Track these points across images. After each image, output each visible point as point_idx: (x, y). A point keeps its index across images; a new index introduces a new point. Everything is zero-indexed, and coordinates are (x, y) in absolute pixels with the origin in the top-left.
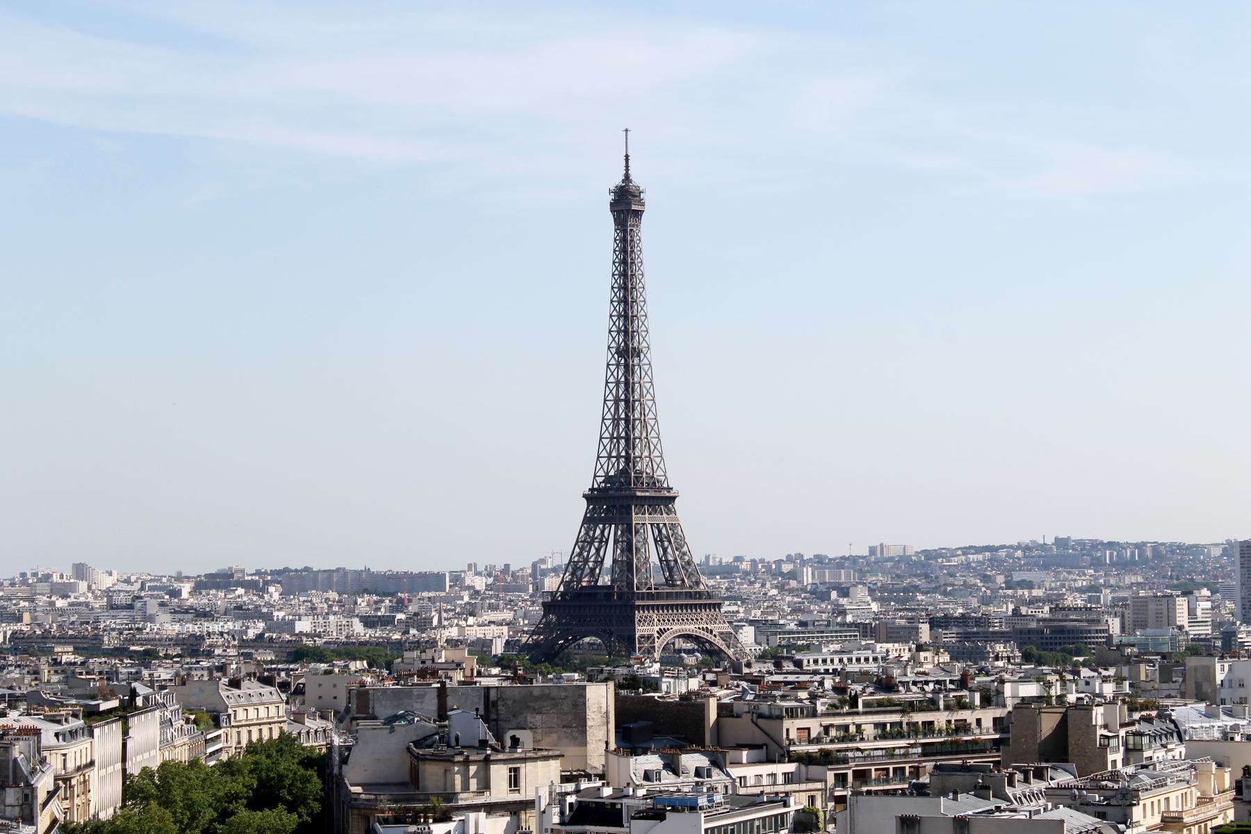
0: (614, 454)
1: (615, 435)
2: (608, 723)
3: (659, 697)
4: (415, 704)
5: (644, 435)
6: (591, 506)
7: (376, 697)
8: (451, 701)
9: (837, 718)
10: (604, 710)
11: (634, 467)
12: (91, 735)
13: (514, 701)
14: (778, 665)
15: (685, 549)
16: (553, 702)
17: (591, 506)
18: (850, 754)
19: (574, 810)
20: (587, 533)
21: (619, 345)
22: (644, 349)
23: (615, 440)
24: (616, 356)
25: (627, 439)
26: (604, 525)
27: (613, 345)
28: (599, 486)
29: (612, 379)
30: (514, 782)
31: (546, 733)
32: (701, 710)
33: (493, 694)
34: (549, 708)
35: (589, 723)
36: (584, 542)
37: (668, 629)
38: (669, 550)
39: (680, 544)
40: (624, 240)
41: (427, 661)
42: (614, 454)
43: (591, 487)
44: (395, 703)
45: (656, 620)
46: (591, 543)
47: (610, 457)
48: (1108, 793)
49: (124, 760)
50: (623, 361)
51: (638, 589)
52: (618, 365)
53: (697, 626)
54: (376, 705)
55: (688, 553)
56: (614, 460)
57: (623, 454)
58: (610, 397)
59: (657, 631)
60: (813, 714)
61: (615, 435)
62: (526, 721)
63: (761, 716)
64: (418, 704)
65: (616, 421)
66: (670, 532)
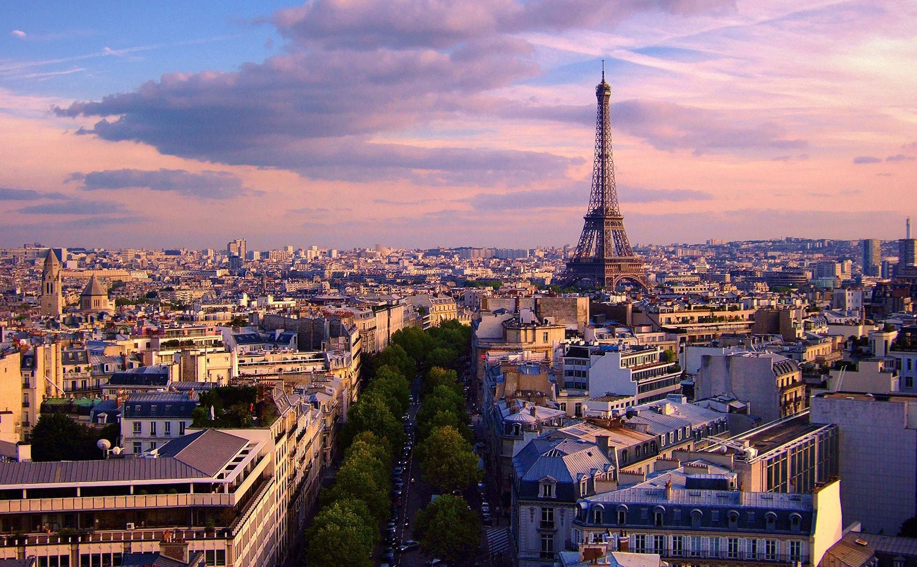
0: (597, 200)
2: (586, 314)
12: (375, 316)
15: (626, 241)
18: (688, 329)
20: (585, 234)
25: (602, 193)
29: (596, 168)
30: (546, 338)
32: (625, 309)
36: (584, 238)
39: (624, 238)
40: (602, 108)
42: (597, 200)
47: (595, 201)
48: (792, 347)
49: (389, 326)
52: (599, 162)
58: (595, 176)
60: (672, 312)
63: (650, 312)
65: (598, 186)
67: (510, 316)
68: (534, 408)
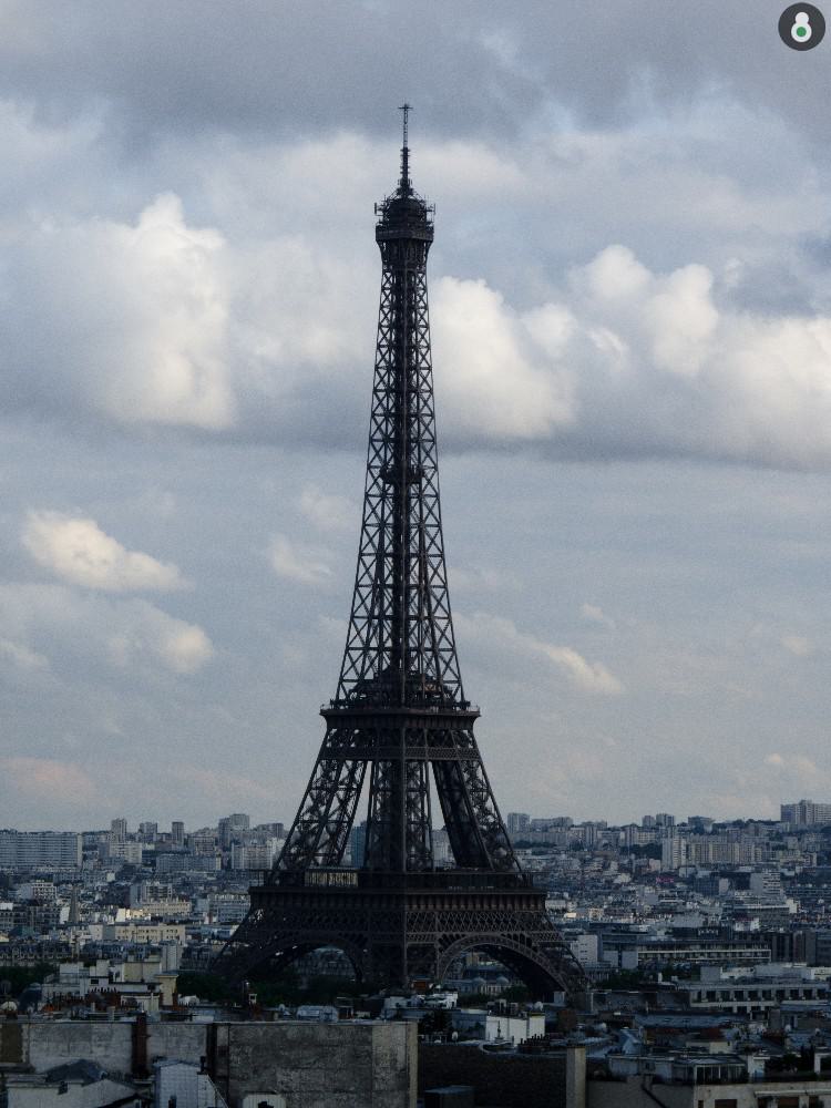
0: (374, 644)
1: (376, 612)
2: (405, 1086)
4: (94, 1049)
6: (334, 731)
7: (33, 1035)
8: (154, 1046)
9: (781, 1085)
10: (400, 1066)
11: (407, 665)
13: (257, 1048)
15: (489, 804)
16: (320, 1050)
17: (334, 731)
20: (326, 775)
21: (386, 463)
22: (427, 471)
23: (376, 621)
24: (380, 481)
25: (396, 619)
26: (355, 762)
27: (377, 462)
28: (348, 696)
29: (373, 520)
31: (307, 1100)
33: (222, 1034)
34: (312, 1061)
36: (321, 790)
37: (458, 937)
40: (397, 289)
41: (101, 981)
42: (374, 644)
43: (334, 698)
44: (63, 1046)
45: (438, 921)
46: (332, 792)
47: (366, 648)
50: (391, 491)
51: (408, 869)
52: (383, 496)
54: (32, 1049)
55: (493, 812)
56: (373, 654)
57: (389, 644)
58: (370, 549)
59: (440, 941)
60: (743, 1078)
61: (376, 612)
63: (658, 1080)
64: (102, 1049)
65: (378, 588)
66: (466, 776)
67: (119, 1091)
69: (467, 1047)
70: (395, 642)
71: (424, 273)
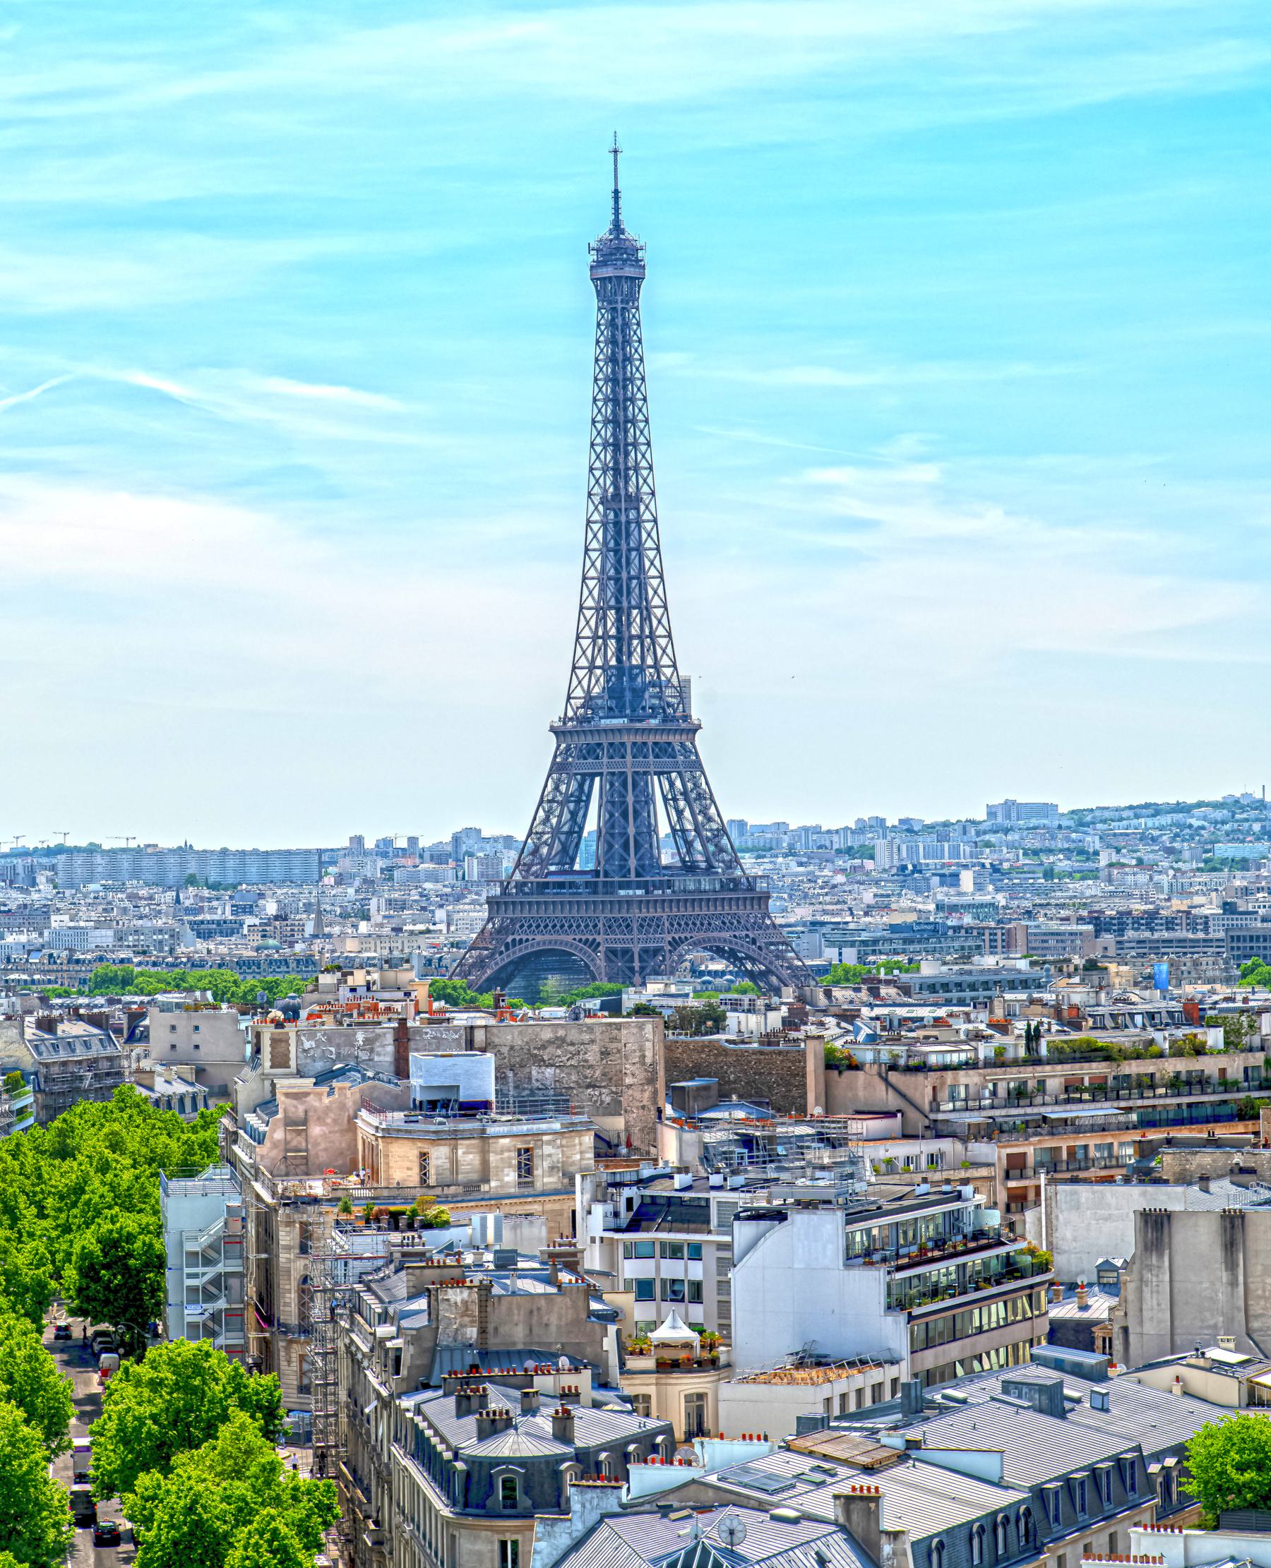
0: (599, 662)
1: (600, 633)
3: (727, 1041)
5: (647, 632)
10: (648, 1060)
13: (512, 1048)
14: (874, 992)
15: (712, 811)
16: (571, 1048)
17: (563, 746)
19: (635, 1208)
20: (557, 788)
23: (600, 641)
24: (601, 508)
25: (619, 639)
27: (596, 490)
34: (564, 1059)
35: (628, 1081)
38: (687, 814)
40: (612, 324)
42: (599, 662)
45: (667, 924)
47: (591, 668)
50: (611, 516)
53: (732, 933)
55: (717, 818)
61: (600, 633)
62: (530, 1079)
65: (601, 611)
66: (690, 785)
68: (567, 1412)
69: (710, 1042)
70: (619, 660)
71: (637, 309)
